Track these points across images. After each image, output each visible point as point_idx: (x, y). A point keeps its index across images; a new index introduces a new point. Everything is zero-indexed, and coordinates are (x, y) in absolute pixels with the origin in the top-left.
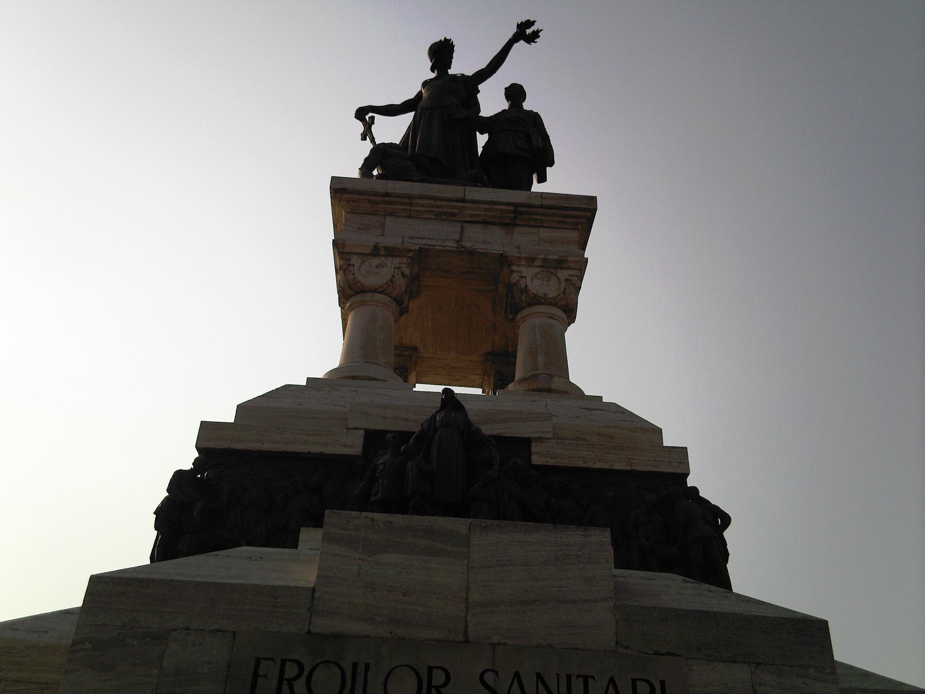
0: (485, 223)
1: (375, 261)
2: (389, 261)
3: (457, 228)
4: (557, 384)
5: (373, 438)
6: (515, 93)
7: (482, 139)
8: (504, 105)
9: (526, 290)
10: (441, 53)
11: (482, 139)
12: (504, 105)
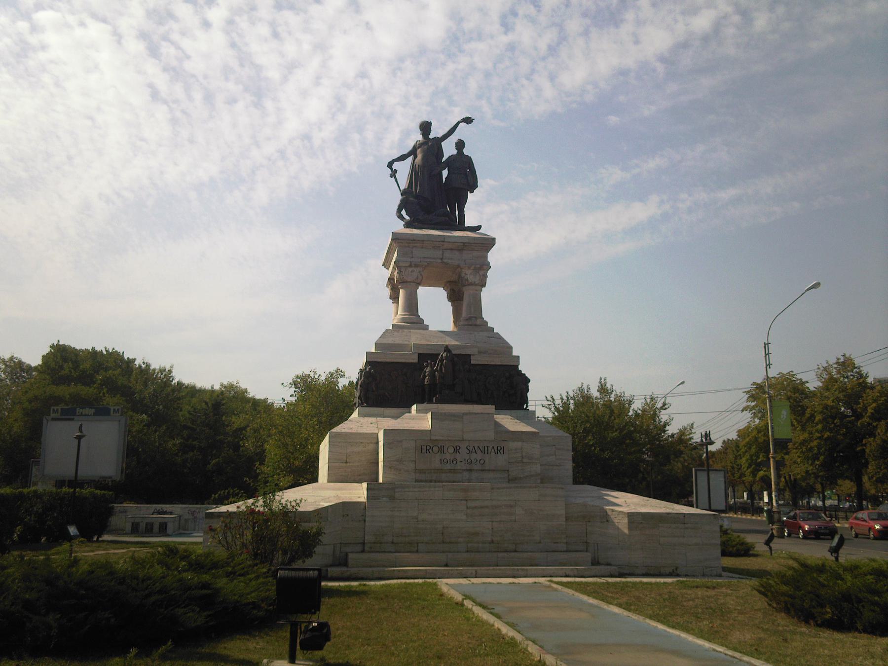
0: (452, 249)
1: (410, 269)
2: (415, 269)
3: (441, 252)
4: (478, 322)
5: (422, 357)
6: (460, 145)
7: (445, 173)
8: (455, 152)
9: (467, 280)
10: (425, 127)
11: (445, 173)
12: (455, 152)
